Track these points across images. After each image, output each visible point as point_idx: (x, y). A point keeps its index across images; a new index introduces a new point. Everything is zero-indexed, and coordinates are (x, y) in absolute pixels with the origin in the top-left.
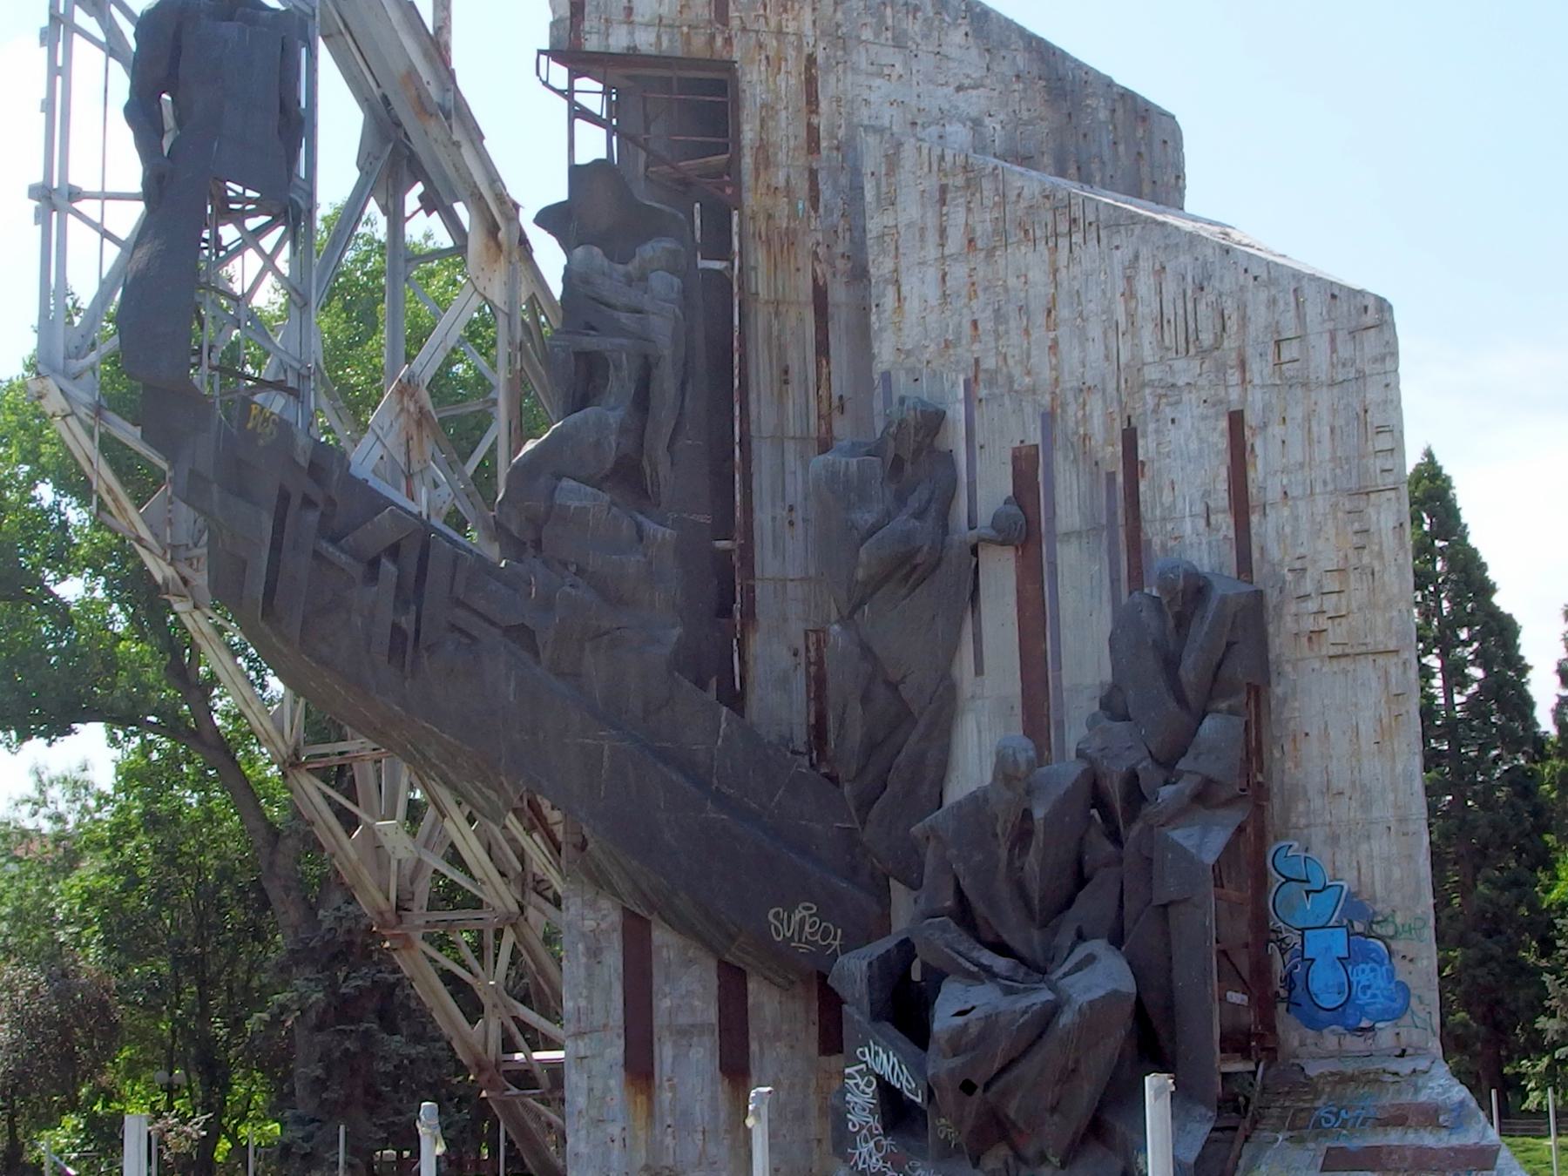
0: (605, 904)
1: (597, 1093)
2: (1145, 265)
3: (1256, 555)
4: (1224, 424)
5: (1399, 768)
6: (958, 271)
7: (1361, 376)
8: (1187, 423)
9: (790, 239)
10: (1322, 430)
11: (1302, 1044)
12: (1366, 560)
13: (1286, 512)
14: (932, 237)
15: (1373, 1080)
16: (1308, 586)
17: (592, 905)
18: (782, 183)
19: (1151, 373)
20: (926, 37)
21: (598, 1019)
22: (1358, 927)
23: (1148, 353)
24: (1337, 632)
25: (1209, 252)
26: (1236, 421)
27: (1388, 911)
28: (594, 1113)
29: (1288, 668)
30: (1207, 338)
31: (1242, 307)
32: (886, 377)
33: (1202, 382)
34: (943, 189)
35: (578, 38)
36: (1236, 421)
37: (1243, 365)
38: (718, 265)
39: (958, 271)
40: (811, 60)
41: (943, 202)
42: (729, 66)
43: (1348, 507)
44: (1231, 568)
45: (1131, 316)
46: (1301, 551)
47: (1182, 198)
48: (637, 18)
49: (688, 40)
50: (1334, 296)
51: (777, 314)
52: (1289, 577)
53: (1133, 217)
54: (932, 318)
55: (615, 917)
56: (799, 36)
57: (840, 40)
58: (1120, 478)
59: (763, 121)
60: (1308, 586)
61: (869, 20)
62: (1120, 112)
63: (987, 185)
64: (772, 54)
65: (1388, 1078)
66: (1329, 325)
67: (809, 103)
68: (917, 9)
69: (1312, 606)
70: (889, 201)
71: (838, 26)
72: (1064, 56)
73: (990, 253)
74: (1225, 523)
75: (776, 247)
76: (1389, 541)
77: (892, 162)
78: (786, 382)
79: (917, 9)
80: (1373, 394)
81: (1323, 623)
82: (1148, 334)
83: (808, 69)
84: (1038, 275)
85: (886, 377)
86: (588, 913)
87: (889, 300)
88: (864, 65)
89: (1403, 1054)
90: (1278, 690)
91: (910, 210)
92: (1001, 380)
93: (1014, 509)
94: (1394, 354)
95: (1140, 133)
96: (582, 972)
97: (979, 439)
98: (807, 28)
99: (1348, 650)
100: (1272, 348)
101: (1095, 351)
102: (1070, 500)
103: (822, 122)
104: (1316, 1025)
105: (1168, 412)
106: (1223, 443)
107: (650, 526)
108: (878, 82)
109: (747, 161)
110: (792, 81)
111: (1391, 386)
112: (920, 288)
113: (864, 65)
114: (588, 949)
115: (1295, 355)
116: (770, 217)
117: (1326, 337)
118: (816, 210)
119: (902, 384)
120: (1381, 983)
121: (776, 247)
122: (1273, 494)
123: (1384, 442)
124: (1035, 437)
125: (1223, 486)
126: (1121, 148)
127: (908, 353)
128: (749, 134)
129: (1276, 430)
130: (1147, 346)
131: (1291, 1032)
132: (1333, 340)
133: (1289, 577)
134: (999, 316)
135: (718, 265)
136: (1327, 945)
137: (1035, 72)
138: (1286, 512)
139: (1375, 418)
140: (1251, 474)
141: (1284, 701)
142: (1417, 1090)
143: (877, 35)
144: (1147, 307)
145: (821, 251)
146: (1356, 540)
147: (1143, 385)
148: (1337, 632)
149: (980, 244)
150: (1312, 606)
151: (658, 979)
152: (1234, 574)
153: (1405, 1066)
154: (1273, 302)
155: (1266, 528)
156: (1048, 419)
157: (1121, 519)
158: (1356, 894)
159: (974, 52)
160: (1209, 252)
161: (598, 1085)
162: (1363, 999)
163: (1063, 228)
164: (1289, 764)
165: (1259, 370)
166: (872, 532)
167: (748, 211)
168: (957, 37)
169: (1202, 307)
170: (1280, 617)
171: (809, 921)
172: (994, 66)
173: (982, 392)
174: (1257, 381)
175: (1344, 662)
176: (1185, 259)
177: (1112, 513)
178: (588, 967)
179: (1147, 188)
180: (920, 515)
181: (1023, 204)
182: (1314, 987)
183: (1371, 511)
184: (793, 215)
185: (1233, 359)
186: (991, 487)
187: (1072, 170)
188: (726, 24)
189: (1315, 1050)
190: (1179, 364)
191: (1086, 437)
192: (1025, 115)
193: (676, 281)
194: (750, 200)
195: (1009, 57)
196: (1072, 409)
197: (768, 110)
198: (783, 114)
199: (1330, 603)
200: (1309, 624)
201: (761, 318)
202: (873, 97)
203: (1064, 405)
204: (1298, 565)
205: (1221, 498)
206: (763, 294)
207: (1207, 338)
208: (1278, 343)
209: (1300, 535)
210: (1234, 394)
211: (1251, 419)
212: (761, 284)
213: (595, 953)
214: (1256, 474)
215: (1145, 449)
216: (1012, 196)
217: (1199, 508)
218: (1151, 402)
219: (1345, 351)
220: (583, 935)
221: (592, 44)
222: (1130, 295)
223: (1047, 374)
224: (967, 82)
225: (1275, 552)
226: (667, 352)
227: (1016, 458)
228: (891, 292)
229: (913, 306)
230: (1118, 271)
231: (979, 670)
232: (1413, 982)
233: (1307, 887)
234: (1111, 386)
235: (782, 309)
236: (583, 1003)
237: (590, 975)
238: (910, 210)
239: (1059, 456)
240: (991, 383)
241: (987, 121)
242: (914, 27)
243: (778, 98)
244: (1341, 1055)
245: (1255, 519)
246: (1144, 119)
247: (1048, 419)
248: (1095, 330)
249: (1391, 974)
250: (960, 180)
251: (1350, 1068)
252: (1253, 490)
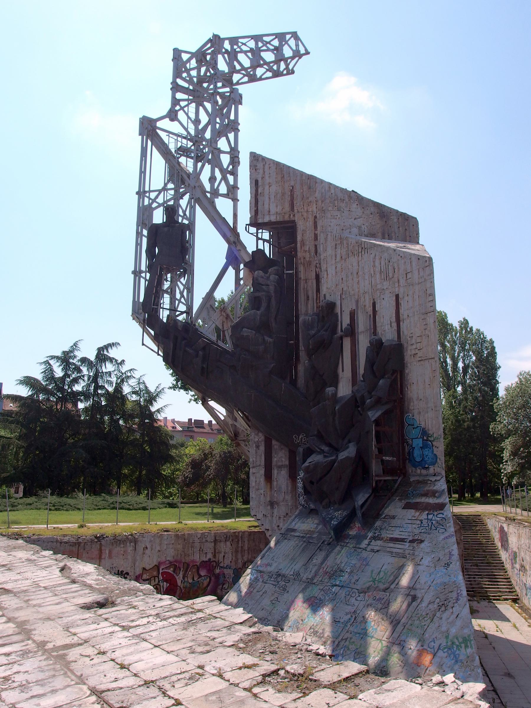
0: (260, 434)
1: (258, 482)
2: (377, 257)
3: (401, 334)
4: (394, 298)
5: (435, 391)
6: (339, 266)
7: (425, 280)
8: (386, 299)
9: (309, 263)
10: (416, 297)
11: (412, 472)
12: (427, 332)
13: (408, 321)
14: (334, 258)
15: (425, 482)
16: (413, 341)
17: (257, 435)
18: (307, 249)
19: (379, 286)
20: (346, 207)
21: (258, 463)
22: (425, 438)
23: (378, 281)
24: (420, 354)
25: (391, 251)
26: (397, 296)
27: (432, 433)
28: (257, 487)
29: (409, 365)
30: (391, 275)
31: (398, 265)
33: (390, 287)
34: (336, 245)
35: (256, 220)
36: (397, 296)
37: (398, 280)
38: (291, 272)
39: (339, 266)
40: (316, 217)
41: (336, 248)
42: (294, 222)
43: (422, 318)
44: (396, 339)
45: (374, 271)
46: (412, 331)
47: (419, 239)
48: (271, 213)
49: (284, 217)
50: (419, 259)
51: (306, 282)
52: (409, 339)
53: (375, 245)
55: (263, 438)
56: (312, 211)
57: (323, 211)
59: (303, 234)
60: (413, 341)
61: (331, 205)
62: (400, 219)
63: (345, 242)
64: (305, 217)
65: (429, 482)
66: (418, 267)
67: (315, 228)
68: (344, 200)
69: (414, 347)
70: (325, 250)
71: (323, 207)
72: (384, 206)
73: (345, 260)
74: (395, 325)
75: (306, 265)
76: (432, 326)
77: (326, 239)
78: (308, 300)
79: (344, 200)
80: (428, 285)
81: (417, 351)
82: (378, 276)
83: (314, 220)
84: (355, 264)
85: (325, 295)
86: (256, 437)
87: (325, 276)
88: (329, 216)
89: (434, 475)
90: (407, 371)
91: (330, 251)
92: (348, 293)
93: (349, 327)
94: (433, 273)
95: (406, 224)
96: (254, 452)
97: (343, 310)
98: (315, 209)
99: (423, 359)
100: (405, 275)
101: (367, 282)
102: (362, 324)
103: (318, 232)
104: (415, 467)
105: (382, 297)
106: (394, 304)
107: (266, 338)
108: (333, 220)
109: (299, 245)
110: (311, 223)
111: (432, 282)
112: (331, 271)
113: (329, 216)
114: (256, 446)
115: (410, 277)
116: (304, 258)
117: (417, 270)
118: (316, 255)
119: (328, 298)
120: (430, 454)
121: (306, 265)
122: (405, 316)
123: (430, 298)
124: (354, 308)
126: (401, 228)
127: (329, 289)
128: (299, 238)
129: (406, 298)
130: (378, 279)
131: (410, 469)
132: (419, 271)
133: (409, 339)
134: (347, 276)
135: (291, 272)
136: (418, 443)
137: (376, 212)
138: (408, 321)
139: (429, 292)
140: (400, 311)
141: (408, 374)
142: (435, 485)
143: (333, 208)
144: (378, 269)
145: (318, 265)
146: (425, 327)
147: (377, 290)
148: (420, 354)
149: (343, 258)
150: (414, 347)
151: (273, 454)
152: (397, 340)
153: (433, 479)
154: (405, 263)
155: (403, 326)
156: (357, 302)
157: (372, 327)
158: (425, 428)
159: (359, 209)
160: (391, 251)
161: (258, 480)
162: (426, 459)
163: (360, 251)
164: (409, 392)
165: (402, 282)
166: (314, 336)
167: (299, 257)
168: (355, 206)
169: (389, 267)
170: (407, 350)
171: (303, 438)
172: (365, 212)
173: (344, 297)
174: (402, 285)
175: (422, 362)
176: (386, 254)
177: (370, 326)
178: (256, 450)
179: (408, 238)
180: (326, 331)
181: (352, 245)
182: (415, 455)
183: (428, 318)
184: (310, 257)
185: (396, 281)
187: (387, 236)
188: (293, 211)
189: (415, 474)
190: (384, 283)
191: (365, 306)
192: (373, 223)
193: (277, 277)
194: (299, 254)
195: (369, 209)
196: (362, 298)
197: (304, 231)
198: (308, 232)
200: (413, 352)
201: (302, 284)
202: (332, 224)
203: (360, 297)
204: (411, 335)
205: (394, 319)
206: (302, 278)
207: (391, 275)
208: (406, 274)
209: (411, 328)
210: (397, 289)
211: (400, 296)
212: (302, 275)
213: (258, 447)
214: (401, 311)
216: (350, 244)
217: (389, 322)
218: (379, 294)
219: (422, 274)
220: (255, 442)
221: (260, 221)
222: (374, 266)
223: (357, 290)
224: (357, 217)
225: (406, 332)
226: (273, 295)
227: (350, 313)
228: (326, 273)
229: (330, 276)
230: (372, 259)
231: (343, 371)
232: (438, 454)
233: (413, 427)
234: (370, 292)
235: (307, 281)
236: (254, 459)
237: (256, 452)
238: (330, 251)
240: (346, 294)
241: (363, 226)
242: (343, 205)
243: (307, 228)
244: (420, 475)
245: (401, 323)
246: (407, 220)
247: (357, 302)
248: (367, 277)
249: (433, 451)
250: (339, 242)
251: (421, 479)
252: (401, 316)
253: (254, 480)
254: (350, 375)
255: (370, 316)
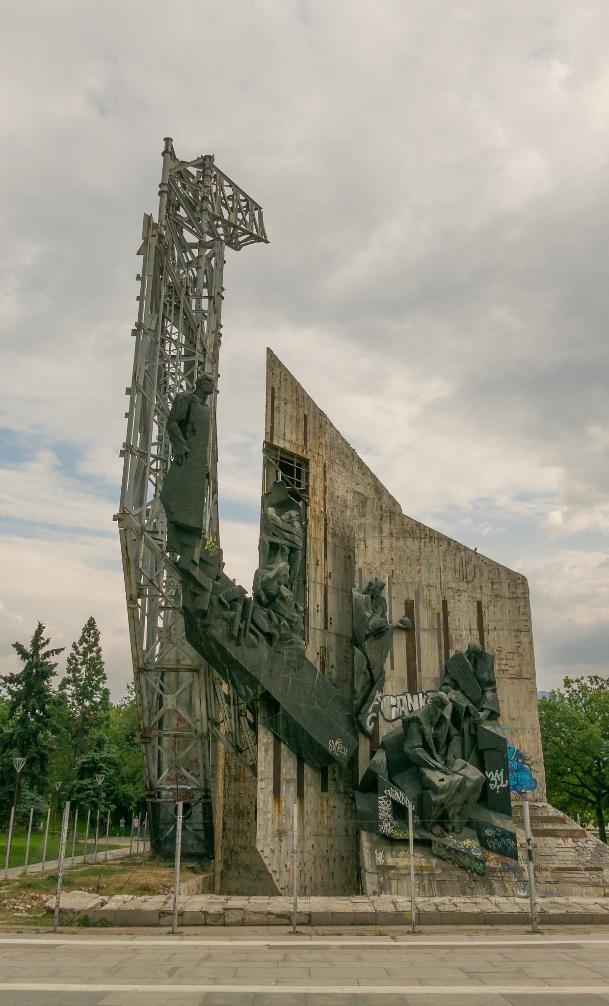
4: (475, 604)
26: (479, 604)
32: (360, 570)
36: (479, 604)
54: (377, 555)
58: (442, 615)
74: (476, 633)
85: (360, 570)
87: (362, 546)
106: (476, 610)
125: (475, 622)
127: (368, 564)
129: (492, 608)
157: (442, 627)
186: (396, 614)
199: (509, 662)
203: (423, 589)
205: (475, 626)
211: (483, 603)
215: (450, 607)
225: (492, 645)
239: (421, 605)
245: (485, 634)
247: (417, 593)
252: (485, 625)
253: (262, 798)
254: (405, 675)
255: (439, 614)
